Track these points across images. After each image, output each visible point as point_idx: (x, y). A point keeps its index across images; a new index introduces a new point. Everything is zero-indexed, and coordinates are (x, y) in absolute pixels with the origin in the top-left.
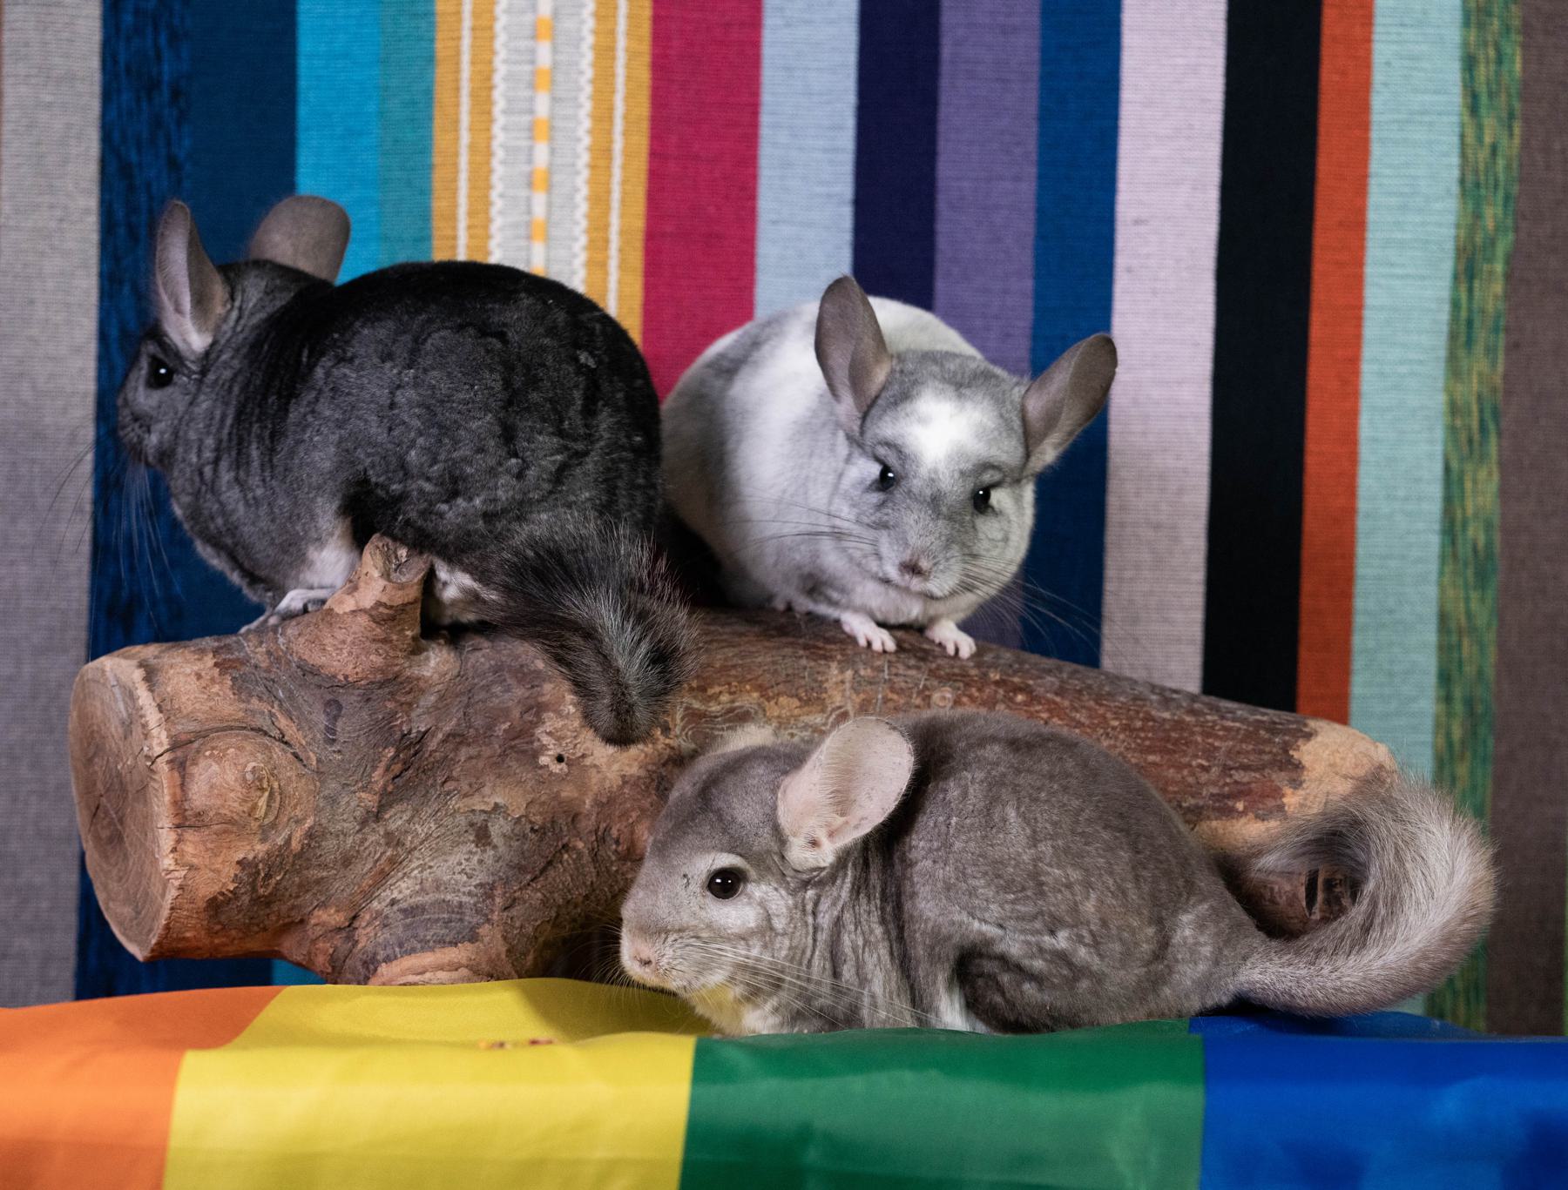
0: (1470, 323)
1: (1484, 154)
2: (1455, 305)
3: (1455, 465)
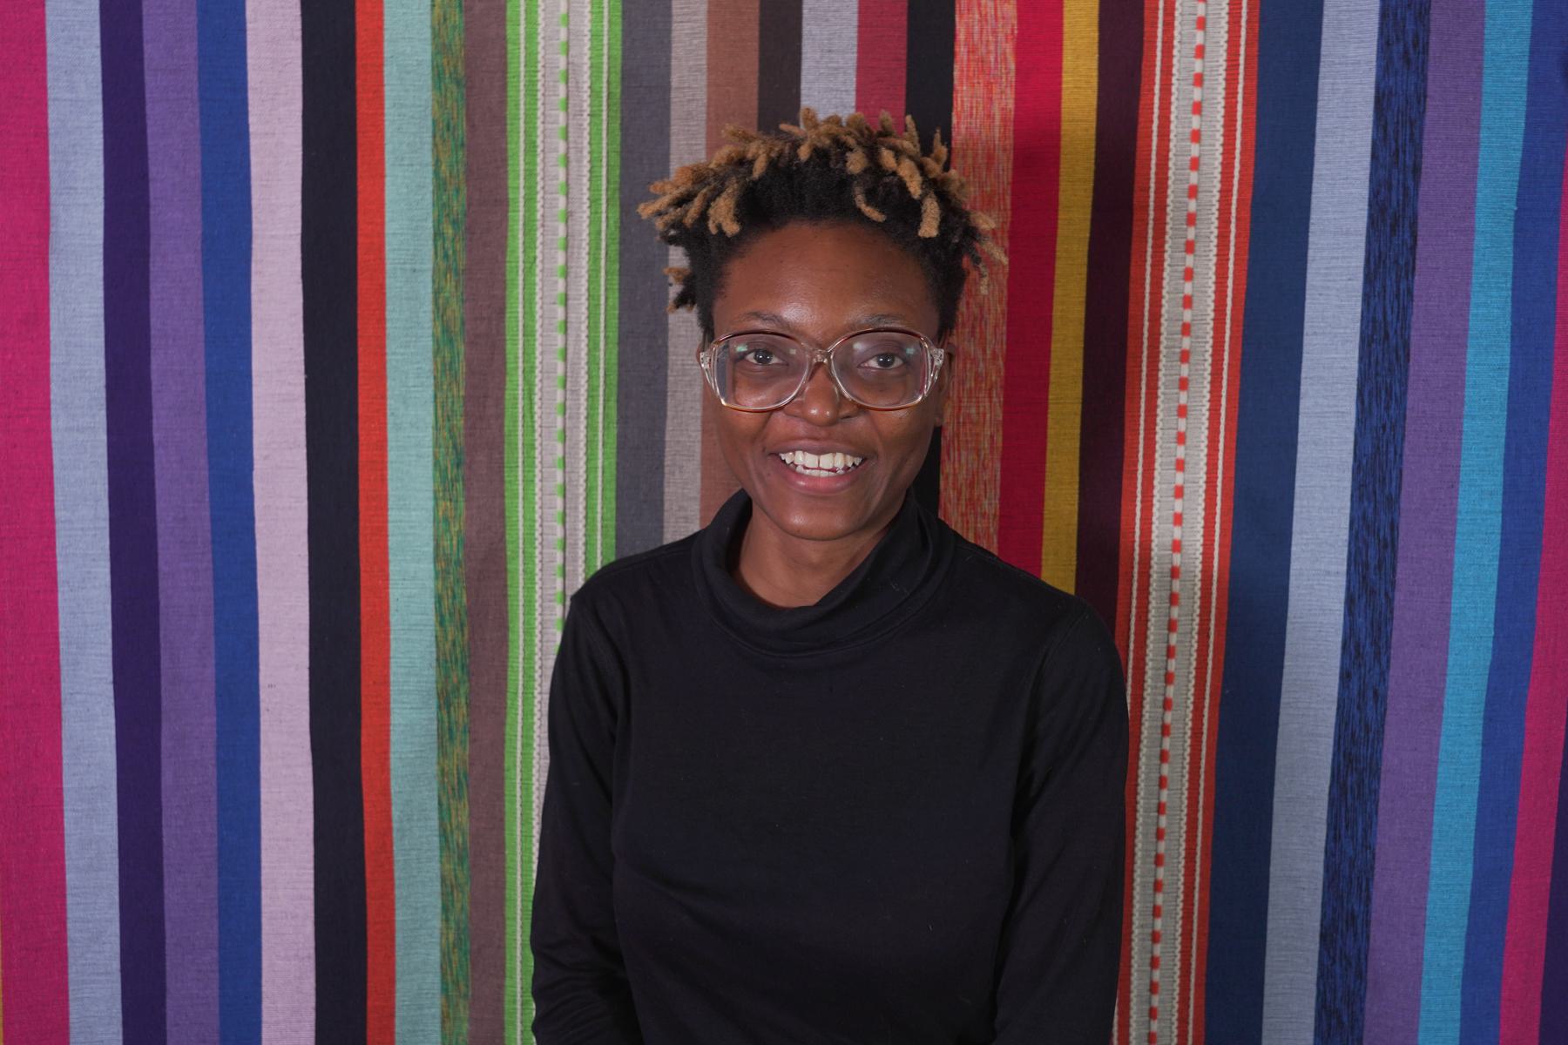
0: (450, 729)
1: (448, 646)
2: (440, 721)
3: (444, 802)
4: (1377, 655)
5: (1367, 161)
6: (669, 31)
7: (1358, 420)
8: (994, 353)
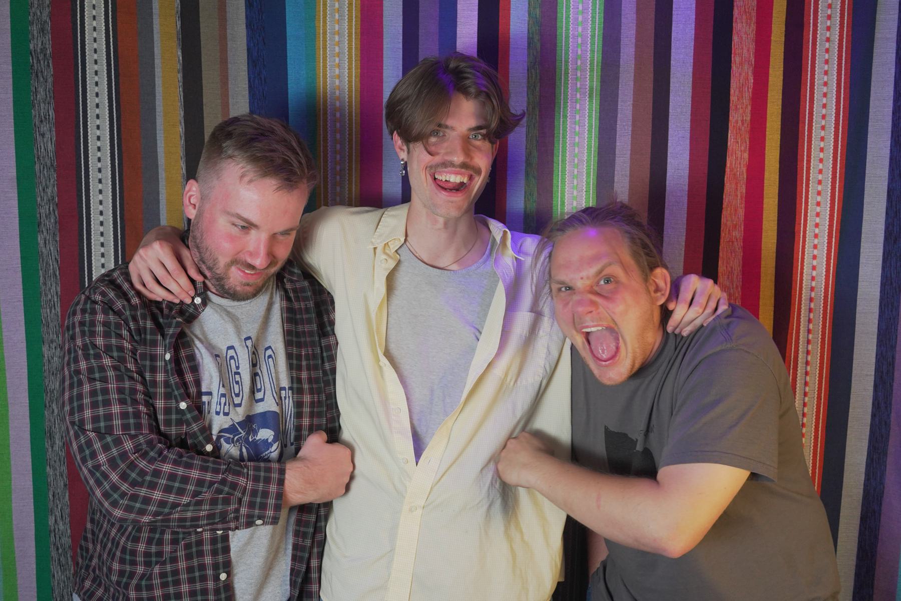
4: (886, 407)
5: (884, 215)
6: (614, 160)
7: (880, 316)
8: (737, 287)
